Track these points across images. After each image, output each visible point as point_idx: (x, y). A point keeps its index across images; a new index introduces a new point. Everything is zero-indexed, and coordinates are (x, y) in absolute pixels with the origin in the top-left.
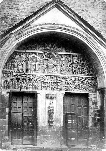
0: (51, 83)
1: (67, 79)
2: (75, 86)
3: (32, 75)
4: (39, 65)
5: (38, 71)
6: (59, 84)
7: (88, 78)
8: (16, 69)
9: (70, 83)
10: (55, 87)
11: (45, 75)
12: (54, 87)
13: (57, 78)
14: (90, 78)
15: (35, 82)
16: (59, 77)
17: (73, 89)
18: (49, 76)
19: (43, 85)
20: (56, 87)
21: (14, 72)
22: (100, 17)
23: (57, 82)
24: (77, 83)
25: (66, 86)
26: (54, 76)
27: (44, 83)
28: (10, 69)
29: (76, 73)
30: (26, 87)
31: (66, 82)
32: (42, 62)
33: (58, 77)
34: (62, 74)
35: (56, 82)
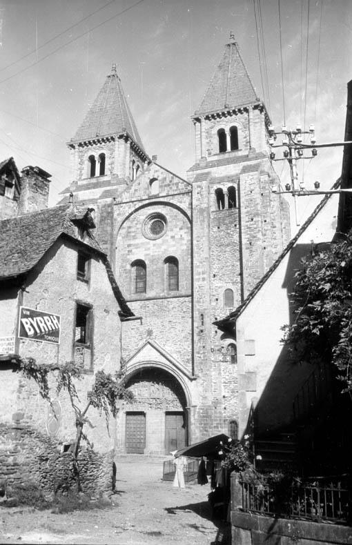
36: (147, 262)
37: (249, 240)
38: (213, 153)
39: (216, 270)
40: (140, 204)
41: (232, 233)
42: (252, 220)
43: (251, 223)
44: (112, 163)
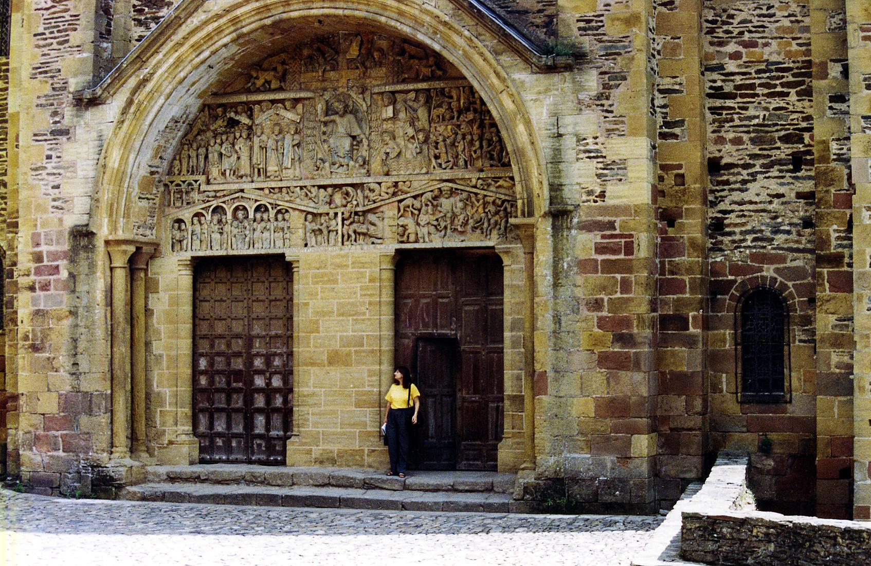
0: (340, 215)
2: (437, 220)
3: (267, 191)
4: (298, 145)
5: (290, 173)
6: (371, 217)
7: (496, 179)
8: (214, 172)
9: (420, 210)
10: (359, 230)
11: (320, 187)
12: (351, 233)
13: (367, 192)
14: (501, 182)
15: (280, 216)
16: (372, 186)
17: (429, 233)
18: (335, 186)
19: (310, 226)
21: (208, 182)
23: (365, 209)
24: (446, 204)
25: (402, 221)
26: (352, 185)
28: (192, 173)
29: (444, 166)
30: (247, 239)
31: (402, 205)
32: (309, 132)
33: (370, 190)
34: (387, 174)
35: (358, 209)
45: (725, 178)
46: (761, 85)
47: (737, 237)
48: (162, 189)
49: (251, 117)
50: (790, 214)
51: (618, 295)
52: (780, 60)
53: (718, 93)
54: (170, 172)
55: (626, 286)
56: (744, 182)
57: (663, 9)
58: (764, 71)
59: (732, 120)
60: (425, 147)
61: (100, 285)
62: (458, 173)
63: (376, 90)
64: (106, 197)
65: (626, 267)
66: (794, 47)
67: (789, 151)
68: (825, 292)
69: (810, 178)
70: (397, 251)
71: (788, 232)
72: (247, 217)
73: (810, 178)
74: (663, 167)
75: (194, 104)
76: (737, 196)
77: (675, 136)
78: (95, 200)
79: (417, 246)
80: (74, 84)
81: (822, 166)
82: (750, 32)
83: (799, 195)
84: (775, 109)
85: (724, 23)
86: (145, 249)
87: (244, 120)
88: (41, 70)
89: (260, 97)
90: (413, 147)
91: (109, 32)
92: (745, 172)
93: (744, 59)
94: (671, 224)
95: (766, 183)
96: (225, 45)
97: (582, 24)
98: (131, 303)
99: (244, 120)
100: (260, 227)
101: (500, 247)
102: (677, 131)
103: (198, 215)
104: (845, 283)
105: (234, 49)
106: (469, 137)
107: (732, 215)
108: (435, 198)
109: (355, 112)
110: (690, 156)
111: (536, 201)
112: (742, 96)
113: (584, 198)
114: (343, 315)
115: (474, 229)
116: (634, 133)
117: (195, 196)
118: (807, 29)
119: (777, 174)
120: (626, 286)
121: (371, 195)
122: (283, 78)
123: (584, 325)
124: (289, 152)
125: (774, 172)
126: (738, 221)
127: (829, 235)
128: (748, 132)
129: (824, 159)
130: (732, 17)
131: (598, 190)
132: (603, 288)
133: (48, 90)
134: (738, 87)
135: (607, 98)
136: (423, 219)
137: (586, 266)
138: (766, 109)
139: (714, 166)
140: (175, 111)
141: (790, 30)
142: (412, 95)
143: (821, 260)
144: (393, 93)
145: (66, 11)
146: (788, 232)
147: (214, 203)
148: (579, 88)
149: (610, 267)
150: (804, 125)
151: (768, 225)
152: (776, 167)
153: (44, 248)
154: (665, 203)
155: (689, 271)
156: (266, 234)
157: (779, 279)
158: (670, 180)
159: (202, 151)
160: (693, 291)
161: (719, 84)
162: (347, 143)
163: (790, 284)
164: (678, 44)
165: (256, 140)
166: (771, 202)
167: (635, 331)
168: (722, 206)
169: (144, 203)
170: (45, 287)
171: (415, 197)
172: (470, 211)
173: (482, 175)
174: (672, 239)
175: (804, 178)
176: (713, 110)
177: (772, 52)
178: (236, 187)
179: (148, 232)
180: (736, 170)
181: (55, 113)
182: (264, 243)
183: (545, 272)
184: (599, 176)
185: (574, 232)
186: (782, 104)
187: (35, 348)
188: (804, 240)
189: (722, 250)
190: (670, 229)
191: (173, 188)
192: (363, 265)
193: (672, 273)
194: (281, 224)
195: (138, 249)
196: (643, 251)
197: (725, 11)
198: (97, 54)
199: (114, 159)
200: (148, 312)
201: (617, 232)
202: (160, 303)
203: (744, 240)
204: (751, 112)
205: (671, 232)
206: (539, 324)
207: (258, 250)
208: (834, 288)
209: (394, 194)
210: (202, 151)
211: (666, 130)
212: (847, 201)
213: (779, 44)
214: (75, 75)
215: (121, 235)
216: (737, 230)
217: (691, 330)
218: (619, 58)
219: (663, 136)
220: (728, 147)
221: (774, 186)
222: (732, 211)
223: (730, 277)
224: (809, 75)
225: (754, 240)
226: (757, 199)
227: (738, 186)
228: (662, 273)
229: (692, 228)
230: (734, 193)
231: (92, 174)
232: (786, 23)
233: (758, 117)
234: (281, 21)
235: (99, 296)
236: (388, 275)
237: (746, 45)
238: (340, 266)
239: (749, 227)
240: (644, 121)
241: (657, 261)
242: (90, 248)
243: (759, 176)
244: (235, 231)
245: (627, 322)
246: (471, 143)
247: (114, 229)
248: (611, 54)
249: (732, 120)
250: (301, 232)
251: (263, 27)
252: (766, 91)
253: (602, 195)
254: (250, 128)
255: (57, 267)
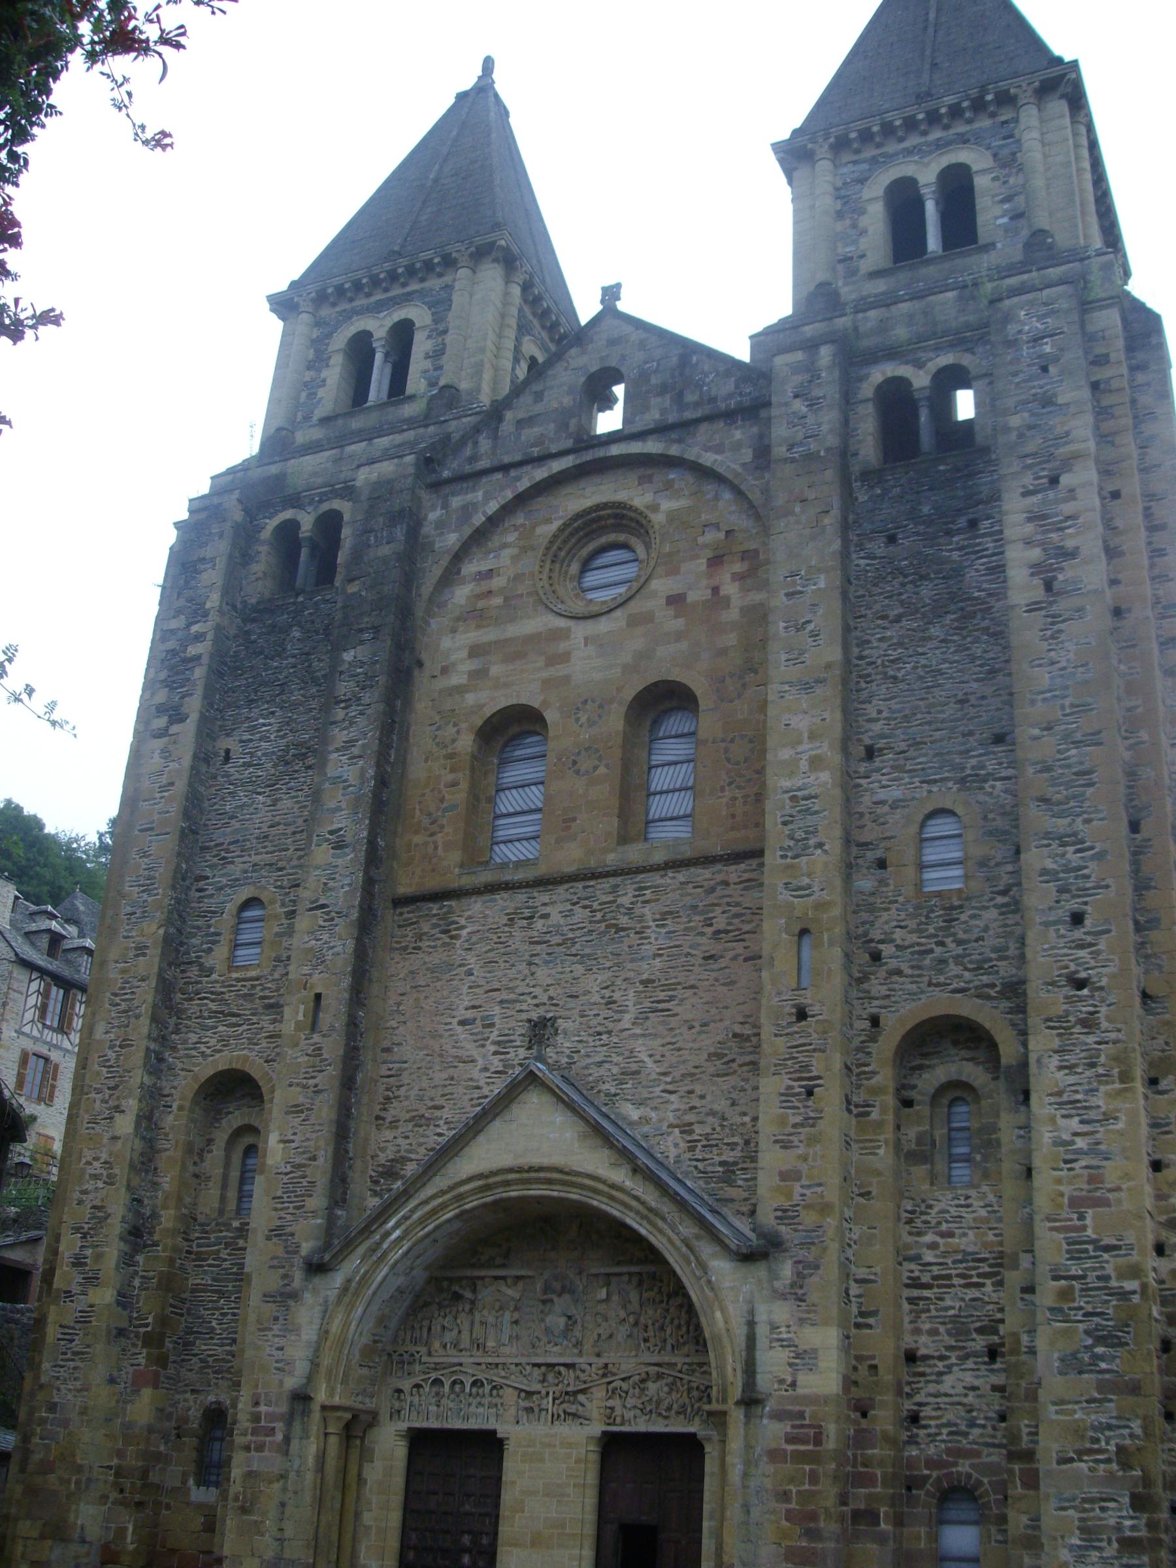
1: (614, 1374)
4: (516, 1322)
5: (506, 1350)
6: (581, 1397)
8: (437, 1345)
11: (534, 1365)
18: (549, 1365)
19: (523, 1404)
20: (572, 1409)
22: (744, 1109)
24: (652, 1387)
25: (610, 1403)
26: (565, 1365)
27: (529, 1394)
31: (611, 1387)
34: (598, 1355)
36: (550, 716)
37: (1036, 569)
38: (865, 266)
39: (877, 727)
40: (540, 474)
41: (955, 555)
42: (1054, 481)
43: (1051, 494)
44: (437, 354)
45: (921, 1369)
46: (958, 1275)
47: (933, 1431)
48: (385, 1358)
49: (474, 1291)
50: (985, 1408)
51: (807, 1487)
52: (976, 1249)
53: (915, 1284)
54: (394, 1341)
55: (814, 1478)
56: (941, 1374)
57: (861, 1200)
58: (961, 1262)
59: (929, 1311)
60: (635, 1331)
61: (312, 1449)
62: (667, 1358)
63: (594, 1271)
64: (326, 1361)
65: (812, 1458)
66: (991, 1237)
67: (983, 1343)
68: (1018, 1489)
69: (1005, 1370)
70: (604, 1433)
71: (983, 1426)
72: (463, 1391)
73: (1005, 1370)
74: (859, 1358)
75: (420, 1275)
76: (932, 1388)
77: (870, 1326)
78: (315, 1364)
79: (626, 1428)
80: (306, 1247)
81: (1013, 1359)
82: (947, 1222)
83: (995, 1388)
84: (973, 1300)
85: (922, 1213)
86: (363, 1417)
87: (468, 1294)
88: (277, 1232)
89: (483, 1273)
90: (624, 1330)
91: (344, 1201)
92: (940, 1364)
93: (942, 1249)
94: (864, 1415)
95: (961, 1375)
96: (449, 1221)
97: (779, 1213)
98: (344, 1471)
99: (468, 1294)
100: (475, 1402)
101: (701, 1434)
102: (871, 1321)
103: (418, 1386)
104: (1032, 1481)
105: (457, 1225)
106: (676, 1322)
107: (928, 1408)
108: (643, 1381)
109: (572, 1292)
110: (882, 1346)
111: (730, 1389)
112: (939, 1286)
113: (776, 1386)
114: (548, 1495)
115: (678, 1413)
116: (826, 1323)
117: (417, 1368)
118: (1000, 1220)
119: (973, 1366)
120: (814, 1478)
121: (582, 1375)
122: (506, 1256)
123: (773, 1517)
124: (507, 1329)
125: (970, 1364)
126: (934, 1414)
127: (1020, 1430)
128: (943, 1323)
129: (1015, 1351)
130: (930, 1207)
131: (789, 1379)
132: (792, 1480)
133: (280, 1251)
134: (934, 1278)
135: (801, 1287)
136: (630, 1402)
137: (775, 1455)
138: (963, 1300)
139: (911, 1357)
140: (400, 1281)
141: (986, 1220)
142: (626, 1278)
143: (1012, 1456)
144: (608, 1275)
145: (304, 1177)
146: (983, 1426)
147: (433, 1376)
148: (774, 1276)
149: (800, 1457)
150: (999, 1316)
151: (962, 1418)
152: (972, 1359)
153: (263, 1408)
154: (856, 1392)
155: (881, 1463)
156: (481, 1410)
157: (975, 1475)
158: (863, 1369)
159: (426, 1323)
160: (884, 1484)
161: (917, 1274)
162: (562, 1321)
163: (985, 1480)
164: (874, 1235)
165: (477, 1316)
166: (966, 1395)
167: (822, 1524)
168: (918, 1398)
169: (365, 1371)
170: (260, 1448)
171: (623, 1380)
172: (674, 1395)
173: (687, 1360)
174: (864, 1430)
175: (998, 1370)
176: (912, 1301)
177: (967, 1242)
178: (456, 1360)
179: (367, 1400)
180: (932, 1362)
181: (285, 1276)
182: (474, 1417)
183: (736, 1460)
184: (790, 1365)
185: (765, 1421)
186: (978, 1294)
187: (244, 1510)
188: (999, 1434)
189: (917, 1443)
190: (863, 1421)
191: (395, 1357)
192: (570, 1445)
193: (866, 1466)
194: (494, 1401)
195: (355, 1417)
196: (831, 1443)
197: (923, 1201)
198: (331, 1220)
199: (335, 1327)
200: (361, 1481)
201: (807, 1422)
202: (374, 1473)
203: (940, 1434)
204: (948, 1303)
205: (864, 1423)
206: (728, 1513)
207: (473, 1424)
208: (1025, 1485)
209: (604, 1375)
210: (426, 1323)
211: (858, 1322)
212: (1032, 1396)
213: (976, 1235)
214: (306, 1240)
215: (337, 1400)
216: (932, 1423)
217: (883, 1525)
218: (813, 1248)
219: (858, 1326)
220: (924, 1339)
221: (969, 1378)
222: (927, 1404)
223: (926, 1472)
224: (1000, 1265)
225: (951, 1433)
226: (952, 1392)
227: (934, 1377)
228: (854, 1466)
229: (884, 1419)
230: (930, 1385)
231: (315, 1338)
232: (983, 1213)
233: (953, 1308)
234: (502, 1200)
235: (311, 1461)
236: (594, 1458)
237: (943, 1235)
238: (549, 1445)
239: (944, 1421)
240: (834, 1312)
241: (850, 1453)
242: (306, 1413)
243: (955, 1369)
244: (451, 1405)
245: (813, 1517)
246: (679, 1327)
247: (331, 1394)
248: (806, 1245)
249: (929, 1311)
250: (513, 1411)
251: (485, 1205)
252: (962, 1282)
253: (793, 1384)
254: (473, 1302)
255: (273, 1429)
